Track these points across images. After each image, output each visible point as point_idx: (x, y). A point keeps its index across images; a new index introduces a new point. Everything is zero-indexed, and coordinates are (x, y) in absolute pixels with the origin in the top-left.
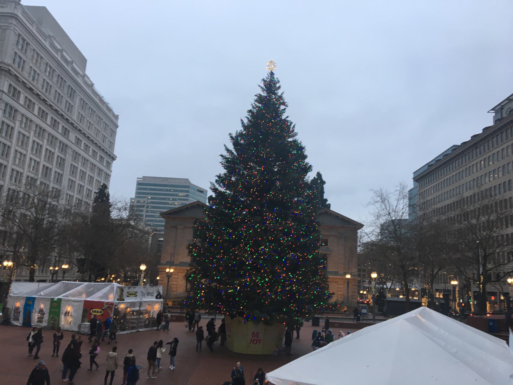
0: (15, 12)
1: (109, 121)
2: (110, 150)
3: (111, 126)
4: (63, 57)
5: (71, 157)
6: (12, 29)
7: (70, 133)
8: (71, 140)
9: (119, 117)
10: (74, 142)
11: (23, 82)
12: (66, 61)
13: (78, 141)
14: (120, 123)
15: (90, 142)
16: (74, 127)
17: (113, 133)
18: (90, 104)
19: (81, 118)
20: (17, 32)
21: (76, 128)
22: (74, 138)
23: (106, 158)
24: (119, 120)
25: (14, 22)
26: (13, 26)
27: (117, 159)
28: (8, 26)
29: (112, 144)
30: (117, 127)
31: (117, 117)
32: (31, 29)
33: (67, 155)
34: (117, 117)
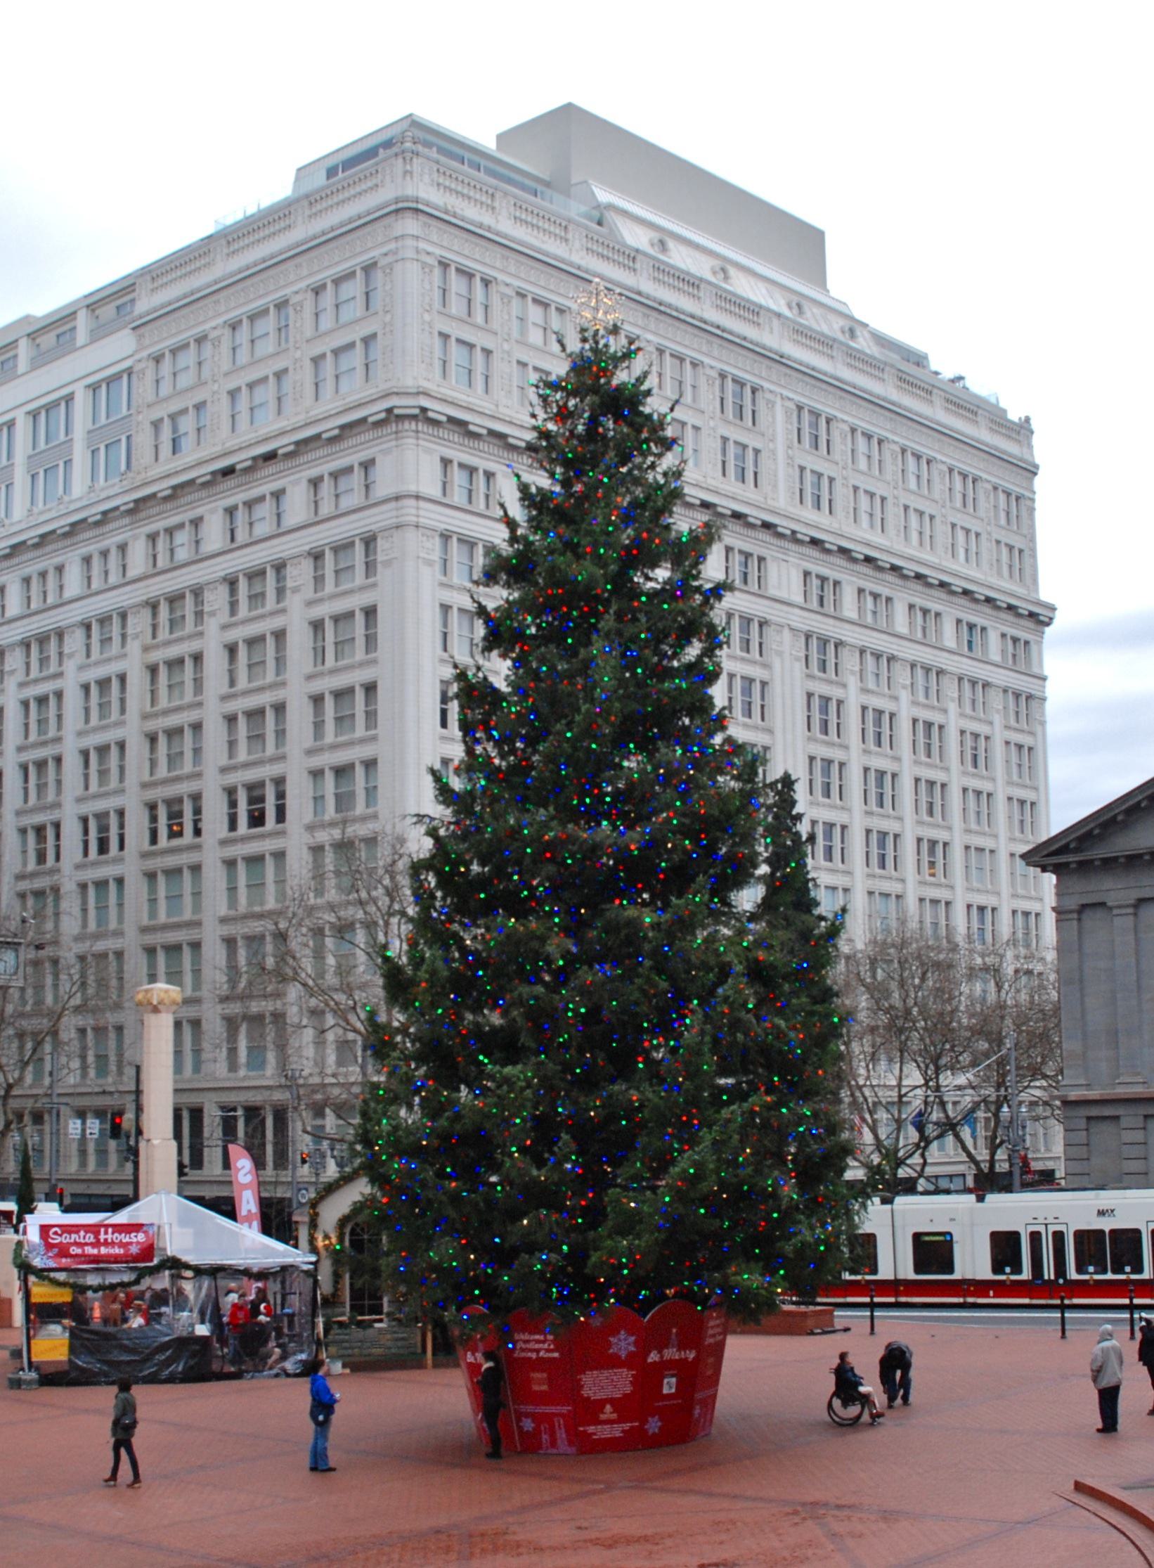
0: (410, 192)
2: (1021, 591)
3: (991, 474)
4: (664, 272)
5: (799, 667)
6: (410, 254)
7: (772, 569)
8: (782, 594)
9: (1034, 425)
10: (799, 599)
11: (452, 420)
12: (691, 283)
13: (823, 592)
14: (1042, 450)
15: (890, 577)
16: (781, 536)
17: (1019, 506)
18: (847, 415)
19: (817, 490)
20: (429, 260)
21: (794, 538)
22: (797, 579)
23: (996, 628)
24: (1036, 440)
25: (410, 225)
26: (410, 242)
28: (395, 252)
29: (1021, 557)
30: (1032, 471)
31: (1023, 430)
33: (777, 664)
34: (1023, 430)
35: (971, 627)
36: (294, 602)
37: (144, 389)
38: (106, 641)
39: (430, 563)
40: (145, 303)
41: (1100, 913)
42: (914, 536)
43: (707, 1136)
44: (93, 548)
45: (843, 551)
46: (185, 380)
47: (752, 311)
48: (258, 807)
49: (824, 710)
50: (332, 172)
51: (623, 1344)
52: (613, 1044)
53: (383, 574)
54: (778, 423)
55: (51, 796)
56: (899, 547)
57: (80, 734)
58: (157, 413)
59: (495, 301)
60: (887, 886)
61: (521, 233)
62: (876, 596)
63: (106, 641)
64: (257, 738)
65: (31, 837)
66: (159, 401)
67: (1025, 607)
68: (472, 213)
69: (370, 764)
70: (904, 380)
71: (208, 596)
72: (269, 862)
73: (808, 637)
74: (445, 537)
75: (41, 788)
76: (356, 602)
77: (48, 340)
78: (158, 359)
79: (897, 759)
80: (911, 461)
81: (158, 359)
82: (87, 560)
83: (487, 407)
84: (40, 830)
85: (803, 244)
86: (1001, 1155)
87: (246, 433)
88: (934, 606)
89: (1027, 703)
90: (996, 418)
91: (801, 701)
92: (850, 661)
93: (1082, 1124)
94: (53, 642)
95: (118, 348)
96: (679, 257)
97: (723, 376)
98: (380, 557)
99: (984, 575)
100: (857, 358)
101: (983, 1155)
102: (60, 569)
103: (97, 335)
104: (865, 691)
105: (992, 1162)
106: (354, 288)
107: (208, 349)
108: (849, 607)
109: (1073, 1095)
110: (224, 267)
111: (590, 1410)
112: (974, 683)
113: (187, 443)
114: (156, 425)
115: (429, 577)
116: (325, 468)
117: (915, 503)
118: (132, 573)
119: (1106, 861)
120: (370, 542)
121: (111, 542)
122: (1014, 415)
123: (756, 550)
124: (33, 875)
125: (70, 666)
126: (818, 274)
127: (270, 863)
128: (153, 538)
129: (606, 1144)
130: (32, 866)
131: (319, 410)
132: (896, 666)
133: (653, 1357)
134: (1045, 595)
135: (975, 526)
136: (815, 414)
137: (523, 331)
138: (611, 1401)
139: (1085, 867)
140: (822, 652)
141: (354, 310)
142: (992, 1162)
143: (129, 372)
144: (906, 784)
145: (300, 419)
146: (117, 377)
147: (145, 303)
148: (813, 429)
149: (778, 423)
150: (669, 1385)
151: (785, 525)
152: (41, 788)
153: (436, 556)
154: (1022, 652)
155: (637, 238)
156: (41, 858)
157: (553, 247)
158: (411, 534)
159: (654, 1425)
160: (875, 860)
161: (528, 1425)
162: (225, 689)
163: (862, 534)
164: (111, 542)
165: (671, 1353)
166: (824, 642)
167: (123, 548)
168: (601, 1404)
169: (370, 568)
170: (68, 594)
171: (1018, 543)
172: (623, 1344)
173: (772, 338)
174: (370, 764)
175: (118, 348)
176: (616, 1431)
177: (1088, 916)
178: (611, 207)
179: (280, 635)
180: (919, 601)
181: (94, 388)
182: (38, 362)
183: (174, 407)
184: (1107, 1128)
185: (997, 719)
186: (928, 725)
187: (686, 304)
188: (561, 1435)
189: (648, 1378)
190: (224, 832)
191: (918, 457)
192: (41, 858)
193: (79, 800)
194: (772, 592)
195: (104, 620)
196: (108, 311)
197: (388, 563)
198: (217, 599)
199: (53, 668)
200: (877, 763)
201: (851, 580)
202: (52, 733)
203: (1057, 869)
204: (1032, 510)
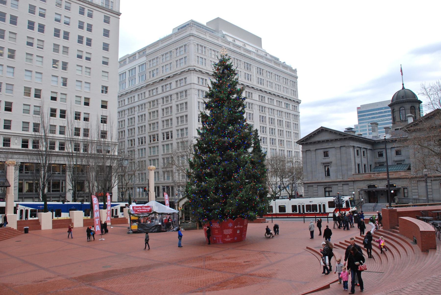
0: (192, 32)
1: (290, 76)
2: (295, 98)
3: (290, 78)
4: (235, 45)
5: (258, 111)
7: (254, 95)
8: (255, 99)
10: (258, 100)
11: (199, 71)
12: (239, 47)
13: (262, 98)
14: (298, 74)
15: (273, 96)
16: (255, 89)
17: (295, 84)
18: (266, 69)
19: (261, 81)
21: (257, 89)
22: (258, 96)
23: (291, 104)
24: (297, 73)
25: (192, 38)
26: (192, 41)
27: (302, 102)
29: (295, 92)
30: (297, 78)
31: (295, 71)
32: (205, 37)
34: (295, 71)
35: (287, 104)
36: (173, 102)
37: (148, 66)
38: (142, 109)
39: (196, 95)
40: (148, 52)
41: (309, 152)
42: (277, 89)
43: (244, 190)
44: (139, 93)
45: (265, 92)
46: (155, 65)
47: (249, 52)
48: (168, 136)
49: (263, 118)
50: (179, 29)
51: (230, 225)
52: (228, 175)
53: (188, 97)
54: (254, 70)
55: (133, 135)
56: (275, 91)
57: (138, 124)
58: (150, 70)
59: (206, 50)
60: (273, 148)
61: (210, 39)
62: (271, 99)
63: (142, 109)
64: (167, 124)
65: (130, 141)
66: (150, 68)
67: (296, 101)
68: (202, 36)
69: (187, 128)
70: (275, 63)
71: (159, 101)
72: (170, 145)
73: (260, 106)
74: (199, 90)
75: (131, 133)
76: (184, 101)
77: (132, 58)
78: (150, 61)
79: (275, 126)
80: (276, 76)
81: (150, 61)
82: (139, 95)
83: (205, 68)
84: (131, 140)
85: (258, 40)
86: (293, 192)
87: (165, 73)
88: (281, 101)
89: (297, 117)
90: (291, 69)
91: (259, 117)
92: (267, 110)
93: (307, 187)
94: (133, 109)
95: (143, 59)
96: (237, 43)
97: (245, 63)
98: (188, 94)
99: (289, 95)
100: (267, 59)
101: (290, 192)
102: (134, 97)
103: (140, 57)
104: (269, 115)
105: (292, 194)
106: (183, 49)
107: (158, 59)
108: (267, 101)
109: (305, 182)
110: (161, 46)
111: (225, 236)
112: (288, 113)
113: (155, 75)
114: (150, 72)
115: (196, 97)
116: (178, 79)
117: (277, 83)
118: (146, 97)
119: (310, 143)
120: (186, 91)
121: (143, 92)
122: (294, 68)
123: (251, 92)
124: (130, 148)
125: (136, 113)
126: (260, 45)
127: (170, 145)
128: (150, 91)
129: (227, 191)
130: (130, 146)
131: (177, 69)
132: (275, 111)
133: (236, 227)
134: (299, 98)
135: (287, 87)
136: (260, 69)
137: (211, 56)
138: (229, 234)
139: (307, 144)
140: (262, 108)
141: (183, 52)
142: (292, 194)
143: (145, 63)
144: (277, 130)
145: (174, 71)
146: (143, 64)
147: (148, 52)
148: (260, 71)
149: (254, 70)
150: (238, 232)
151: (255, 87)
152: (131, 133)
153: (197, 93)
154: (295, 108)
155: (230, 40)
156: (132, 145)
157: (216, 41)
158: (193, 90)
159: (236, 238)
160: (271, 143)
161: (215, 239)
162: (162, 116)
163: (269, 89)
164: (143, 92)
165: (238, 226)
166: (262, 107)
167: (144, 93)
168: (227, 235)
169: (186, 95)
170: (135, 101)
171: (295, 90)
172: (230, 225)
173: (253, 56)
174: (187, 128)
175: (143, 59)
176: (230, 239)
177: (307, 152)
178: (225, 34)
179: (171, 107)
180: (278, 100)
181: (139, 66)
182: (130, 61)
183: (153, 69)
184: (311, 187)
185: (292, 119)
186: (280, 121)
187: (238, 50)
188: (220, 240)
189: (235, 230)
190: (162, 140)
191: (278, 76)
192: (132, 145)
193: (138, 135)
194: (254, 99)
195: (142, 105)
196: (141, 53)
197: (189, 95)
198: (160, 101)
199: (133, 113)
200: (272, 127)
201: (267, 96)
202: (133, 124)
203: (302, 144)
204: (297, 84)
